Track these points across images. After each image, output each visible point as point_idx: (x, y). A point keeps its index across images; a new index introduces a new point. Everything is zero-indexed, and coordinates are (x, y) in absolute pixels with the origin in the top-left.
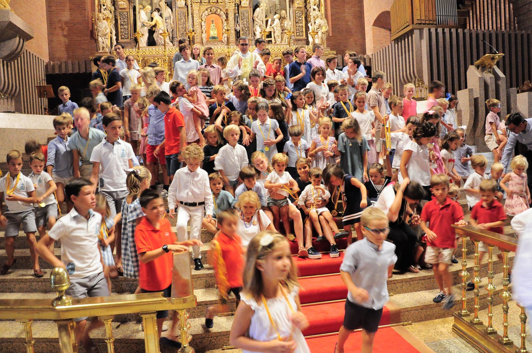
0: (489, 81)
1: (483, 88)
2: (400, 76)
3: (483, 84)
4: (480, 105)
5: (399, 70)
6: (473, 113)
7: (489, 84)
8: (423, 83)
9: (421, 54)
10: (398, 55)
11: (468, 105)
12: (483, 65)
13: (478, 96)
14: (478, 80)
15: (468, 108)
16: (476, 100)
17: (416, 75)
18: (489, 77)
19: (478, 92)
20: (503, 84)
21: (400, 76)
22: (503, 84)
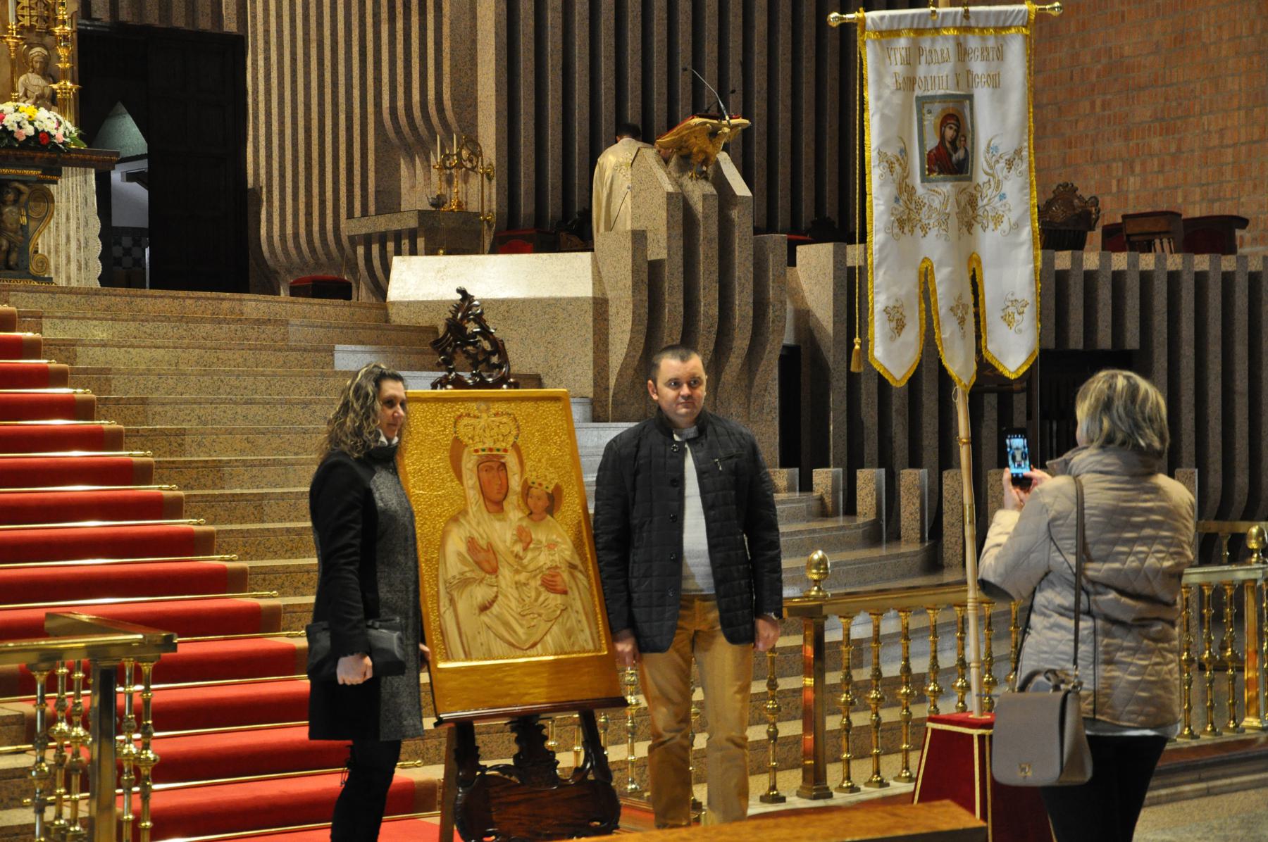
0: (699, 207)
1: (679, 230)
2: (378, 105)
3: (679, 216)
4: (666, 285)
5: (378, 80)
6: (644, 311)
7: (700, 216)
8: (476, 153)
9: (473, 28)
10: (376, 15)
11: (629, 283)
12: (685, 151)
13: (663, 255)
14: (662, 201)
15: (627, 295)
16: (655, 268)
17: (449, 114)
18: (698, 191)
19: (663, 243)
20: (742, 221)
21: (378, 105)
22: (742, 221)
